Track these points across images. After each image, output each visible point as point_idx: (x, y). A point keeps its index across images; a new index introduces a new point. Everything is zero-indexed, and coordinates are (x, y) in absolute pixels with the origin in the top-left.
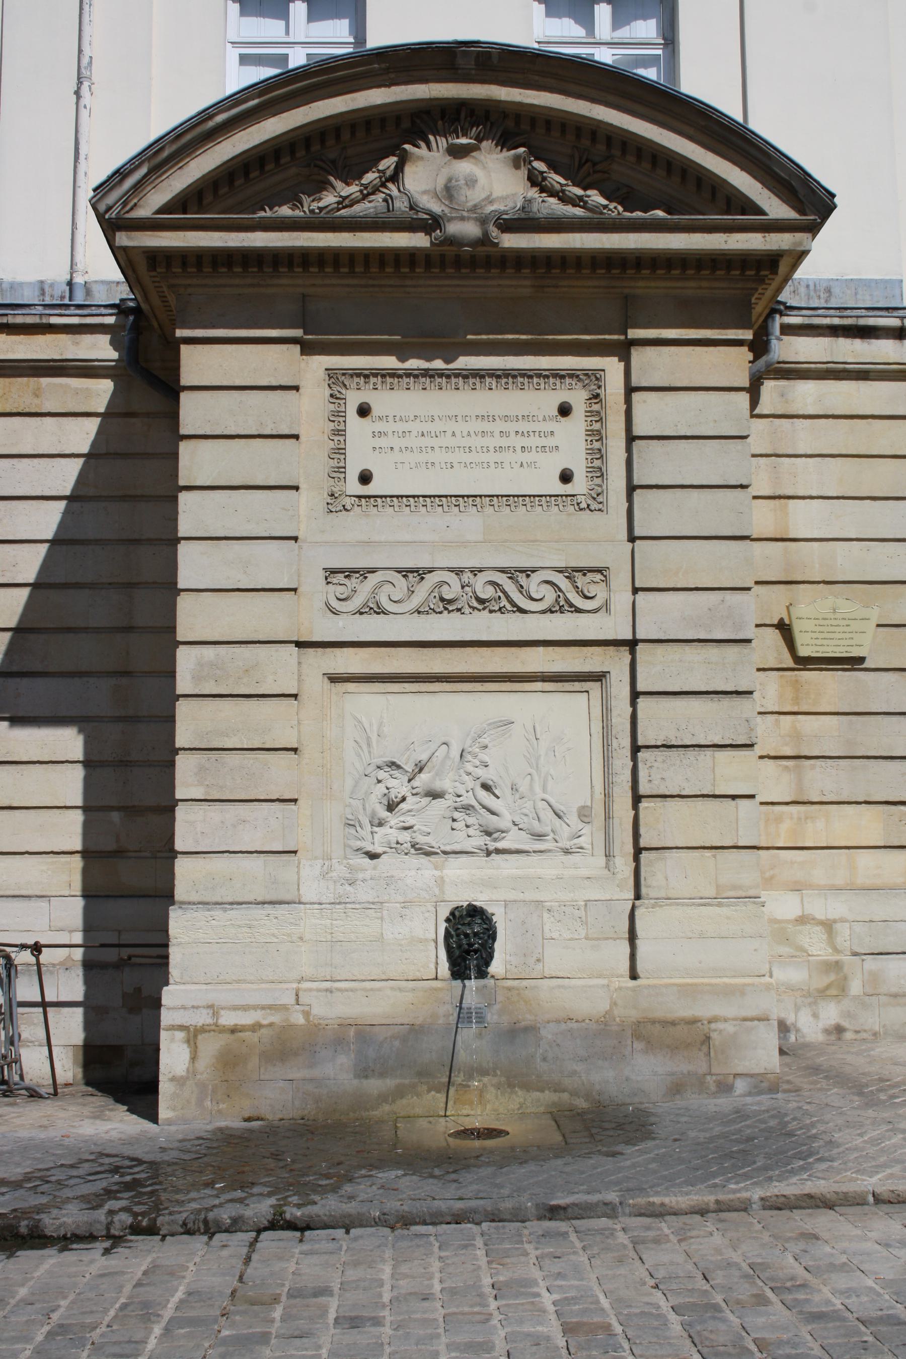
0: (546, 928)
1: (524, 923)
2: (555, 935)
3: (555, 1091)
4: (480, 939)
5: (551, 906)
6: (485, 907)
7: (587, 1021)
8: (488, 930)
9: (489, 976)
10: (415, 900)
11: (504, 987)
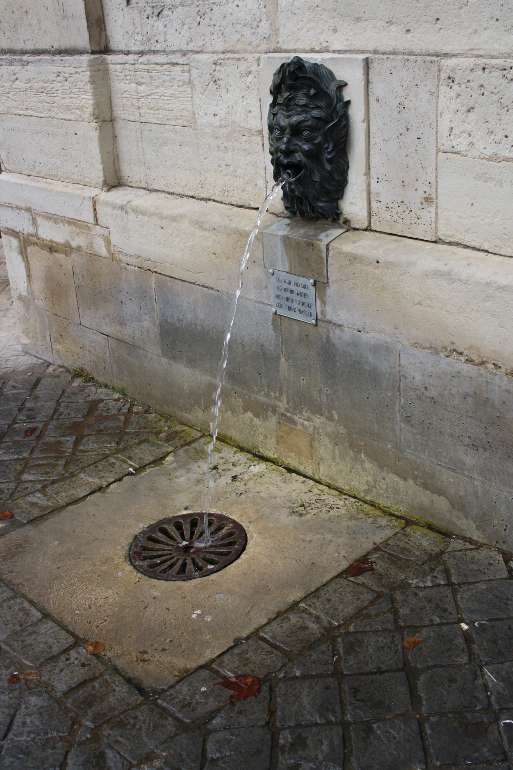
0: (444, 124)
1: (402, 107)
2: (461, 143)
3: (425, 486)
4: (308, 140)
6: (329, 66)
7: (490, 366)
8: (325, 121)
9: (341, 221)
10: (240, 46)
11: (340, 253)
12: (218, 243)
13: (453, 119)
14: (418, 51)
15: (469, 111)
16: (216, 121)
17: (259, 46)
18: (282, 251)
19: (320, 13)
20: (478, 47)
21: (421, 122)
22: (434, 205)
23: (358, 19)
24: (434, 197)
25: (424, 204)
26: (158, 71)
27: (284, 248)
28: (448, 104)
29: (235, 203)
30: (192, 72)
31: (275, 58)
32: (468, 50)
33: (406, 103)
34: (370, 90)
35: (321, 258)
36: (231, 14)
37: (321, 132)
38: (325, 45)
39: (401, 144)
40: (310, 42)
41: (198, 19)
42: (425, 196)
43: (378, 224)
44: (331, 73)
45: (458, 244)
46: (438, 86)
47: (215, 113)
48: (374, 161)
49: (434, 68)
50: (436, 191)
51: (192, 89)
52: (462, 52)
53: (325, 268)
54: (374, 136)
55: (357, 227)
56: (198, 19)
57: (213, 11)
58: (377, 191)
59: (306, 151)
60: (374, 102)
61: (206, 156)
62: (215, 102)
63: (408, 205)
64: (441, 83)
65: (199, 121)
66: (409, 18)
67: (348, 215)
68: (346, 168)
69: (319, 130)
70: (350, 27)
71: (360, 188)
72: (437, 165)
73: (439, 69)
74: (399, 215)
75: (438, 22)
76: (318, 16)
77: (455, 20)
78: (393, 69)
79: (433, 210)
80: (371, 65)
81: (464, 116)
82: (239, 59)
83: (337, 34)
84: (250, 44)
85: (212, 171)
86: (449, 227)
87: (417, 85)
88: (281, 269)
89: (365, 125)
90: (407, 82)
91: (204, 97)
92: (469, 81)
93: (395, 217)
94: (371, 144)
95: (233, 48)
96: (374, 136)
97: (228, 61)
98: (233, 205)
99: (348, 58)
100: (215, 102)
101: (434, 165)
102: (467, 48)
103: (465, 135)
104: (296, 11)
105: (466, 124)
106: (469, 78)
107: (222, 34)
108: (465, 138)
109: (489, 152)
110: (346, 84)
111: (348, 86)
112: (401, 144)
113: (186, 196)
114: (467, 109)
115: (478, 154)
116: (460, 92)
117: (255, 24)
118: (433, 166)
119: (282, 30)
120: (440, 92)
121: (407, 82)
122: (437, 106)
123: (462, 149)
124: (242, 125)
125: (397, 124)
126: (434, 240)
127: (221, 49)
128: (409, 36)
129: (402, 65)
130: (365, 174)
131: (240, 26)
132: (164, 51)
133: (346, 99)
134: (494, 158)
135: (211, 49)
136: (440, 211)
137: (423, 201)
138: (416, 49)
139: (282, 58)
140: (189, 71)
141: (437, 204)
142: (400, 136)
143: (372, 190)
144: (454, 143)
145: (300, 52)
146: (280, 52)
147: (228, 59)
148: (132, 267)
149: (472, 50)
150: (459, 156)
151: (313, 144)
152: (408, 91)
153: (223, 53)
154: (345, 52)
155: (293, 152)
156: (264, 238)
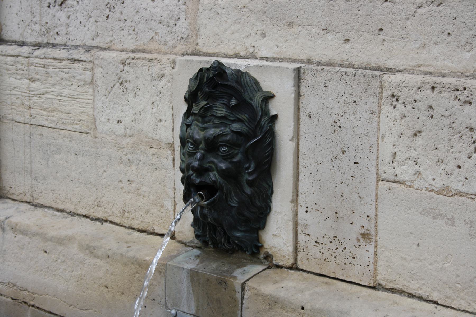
0: (386, 149)
1: (337, 126)
2: (406, 172)
4: (226, 158)
5: (399, 86)
6: (255, 74)
8: (246, 136)
9: (262, 256)
10: (153, 46)
11: (258, 295)
12: (112, 274)
13: (397, 143)
14: (357, 64)
15: (415, 135)
16: (120, 129)
17: (175, 47)
18: (188, 288)
19: (248, 15)
20: (426, 64)
21: (359, 144)
22: (373, 243)
23: (290, 24)
24: (373, 233)
25: (361, 240)
26: (55, 67)
27: (190, 284)
28: (391, 125)
29: (136, 227)
30: (95, 71)
31: (192, 61)
32: (415, 66)
33: (342, 121)
34: (301, 105)
35: (235, 300)
36: (145, 9)
37: (242, 149)
38: (251, 50)
39: (335, 168)
40: (234, 46)
41: (107, 12)
42: (363, 231)
43: (305, 261)
44: (256, 83)
45: (401, 292)
46: (379, 105)
47: (119, 119)
48: (303, 186)
49: (376, 84)
50: (376, 226)
51: (94, 90)
52: (409, 68)
53: (239, 312)
54: (304, 157)
55: (281, 264)
56: (107, 12)
57: (125, 5)
58: (306, 223)
59: (223, 170)
60: (304, 118)
61: (105, 169)
62: (120, 107)
63: (342, 241)
64: (383, 101)
65: (100, 128)
66: (348, 26)
67: (270, 248)
68: (270, 193)
69: (239, 146)
70: (281, 33)
71: (286, 218)
72: (377, 195)
73: (382, 85)
74: (330, 252)
75: (382, 33)
76: (244, 17)
77: (401, 32)
78: (328, 82)
79: (371, 249)
80: (302, 76)
81: (409, 140)
82: (150, 60)
83: (265, 38)
84: (165, 43)
85: (111, 187)
86: (390, 270)
87: (355, 102)
88: (186, 310)
89: (293, 144)
90: (344, 98)
91: (107, 100)
92: (415, 101)
93: (326, 255)
94: (300, 167)
95: (145, 47)
96: (304, 157)
97: (138, 61)
98: (134, 229)
99: (277, 67)
100: (120, 107)
101: (374, 194)
102: (413, 63)
103: (410, 162)
104: (220, 11)
105: (412, 150)
106: (416, 97)
107: (134, 31)
108: (410, 166)
109: (438, 184)
110: (273, 96)
111: (276, 98)
112: (335, 168)
113: (78, 215)
114: (413, 132)
115: (426, 185)
116: (406, 112)
117: (172, 22)
118: (373, 197)
119: (202, 31)
120: (382, 112)
121: (344, 98)
122: (378, 128)
123: (407, 178)
124: (150, 135)
125: (331, 145)
126: (372, 285)
127: (132, 47)
128: (348, 46)
129: (339, 79)
130: (292, 202)
131: (154, 23)
132: (65, 45)
133: (273, 113)
134: (445, 191)
135: (120, 47)
136: (379, 250)
137: (360, 237)
138: (356, 61)
139: (200, 62)
140: (92, 69)
141: (376, 241)
142: (334, 159)
143: (299, 221)
144: (398, 171)
145: (222, 57)
146: (200, 55)
147: (138, 59)
148: (4, 298)
149: (419, 66)
150: (403, 186)
151: (232, 163)
152: (345, 108)
153: (133, 51)
154: (274, 59)
155: (208, 170)
156: (168, 272)
